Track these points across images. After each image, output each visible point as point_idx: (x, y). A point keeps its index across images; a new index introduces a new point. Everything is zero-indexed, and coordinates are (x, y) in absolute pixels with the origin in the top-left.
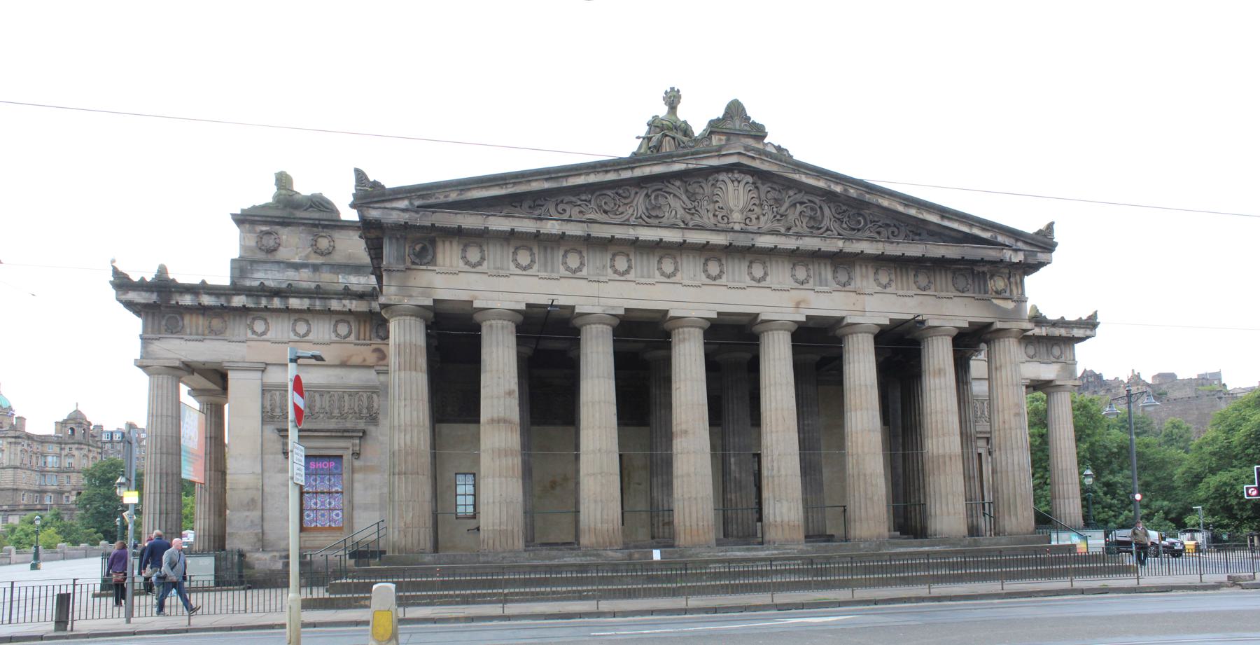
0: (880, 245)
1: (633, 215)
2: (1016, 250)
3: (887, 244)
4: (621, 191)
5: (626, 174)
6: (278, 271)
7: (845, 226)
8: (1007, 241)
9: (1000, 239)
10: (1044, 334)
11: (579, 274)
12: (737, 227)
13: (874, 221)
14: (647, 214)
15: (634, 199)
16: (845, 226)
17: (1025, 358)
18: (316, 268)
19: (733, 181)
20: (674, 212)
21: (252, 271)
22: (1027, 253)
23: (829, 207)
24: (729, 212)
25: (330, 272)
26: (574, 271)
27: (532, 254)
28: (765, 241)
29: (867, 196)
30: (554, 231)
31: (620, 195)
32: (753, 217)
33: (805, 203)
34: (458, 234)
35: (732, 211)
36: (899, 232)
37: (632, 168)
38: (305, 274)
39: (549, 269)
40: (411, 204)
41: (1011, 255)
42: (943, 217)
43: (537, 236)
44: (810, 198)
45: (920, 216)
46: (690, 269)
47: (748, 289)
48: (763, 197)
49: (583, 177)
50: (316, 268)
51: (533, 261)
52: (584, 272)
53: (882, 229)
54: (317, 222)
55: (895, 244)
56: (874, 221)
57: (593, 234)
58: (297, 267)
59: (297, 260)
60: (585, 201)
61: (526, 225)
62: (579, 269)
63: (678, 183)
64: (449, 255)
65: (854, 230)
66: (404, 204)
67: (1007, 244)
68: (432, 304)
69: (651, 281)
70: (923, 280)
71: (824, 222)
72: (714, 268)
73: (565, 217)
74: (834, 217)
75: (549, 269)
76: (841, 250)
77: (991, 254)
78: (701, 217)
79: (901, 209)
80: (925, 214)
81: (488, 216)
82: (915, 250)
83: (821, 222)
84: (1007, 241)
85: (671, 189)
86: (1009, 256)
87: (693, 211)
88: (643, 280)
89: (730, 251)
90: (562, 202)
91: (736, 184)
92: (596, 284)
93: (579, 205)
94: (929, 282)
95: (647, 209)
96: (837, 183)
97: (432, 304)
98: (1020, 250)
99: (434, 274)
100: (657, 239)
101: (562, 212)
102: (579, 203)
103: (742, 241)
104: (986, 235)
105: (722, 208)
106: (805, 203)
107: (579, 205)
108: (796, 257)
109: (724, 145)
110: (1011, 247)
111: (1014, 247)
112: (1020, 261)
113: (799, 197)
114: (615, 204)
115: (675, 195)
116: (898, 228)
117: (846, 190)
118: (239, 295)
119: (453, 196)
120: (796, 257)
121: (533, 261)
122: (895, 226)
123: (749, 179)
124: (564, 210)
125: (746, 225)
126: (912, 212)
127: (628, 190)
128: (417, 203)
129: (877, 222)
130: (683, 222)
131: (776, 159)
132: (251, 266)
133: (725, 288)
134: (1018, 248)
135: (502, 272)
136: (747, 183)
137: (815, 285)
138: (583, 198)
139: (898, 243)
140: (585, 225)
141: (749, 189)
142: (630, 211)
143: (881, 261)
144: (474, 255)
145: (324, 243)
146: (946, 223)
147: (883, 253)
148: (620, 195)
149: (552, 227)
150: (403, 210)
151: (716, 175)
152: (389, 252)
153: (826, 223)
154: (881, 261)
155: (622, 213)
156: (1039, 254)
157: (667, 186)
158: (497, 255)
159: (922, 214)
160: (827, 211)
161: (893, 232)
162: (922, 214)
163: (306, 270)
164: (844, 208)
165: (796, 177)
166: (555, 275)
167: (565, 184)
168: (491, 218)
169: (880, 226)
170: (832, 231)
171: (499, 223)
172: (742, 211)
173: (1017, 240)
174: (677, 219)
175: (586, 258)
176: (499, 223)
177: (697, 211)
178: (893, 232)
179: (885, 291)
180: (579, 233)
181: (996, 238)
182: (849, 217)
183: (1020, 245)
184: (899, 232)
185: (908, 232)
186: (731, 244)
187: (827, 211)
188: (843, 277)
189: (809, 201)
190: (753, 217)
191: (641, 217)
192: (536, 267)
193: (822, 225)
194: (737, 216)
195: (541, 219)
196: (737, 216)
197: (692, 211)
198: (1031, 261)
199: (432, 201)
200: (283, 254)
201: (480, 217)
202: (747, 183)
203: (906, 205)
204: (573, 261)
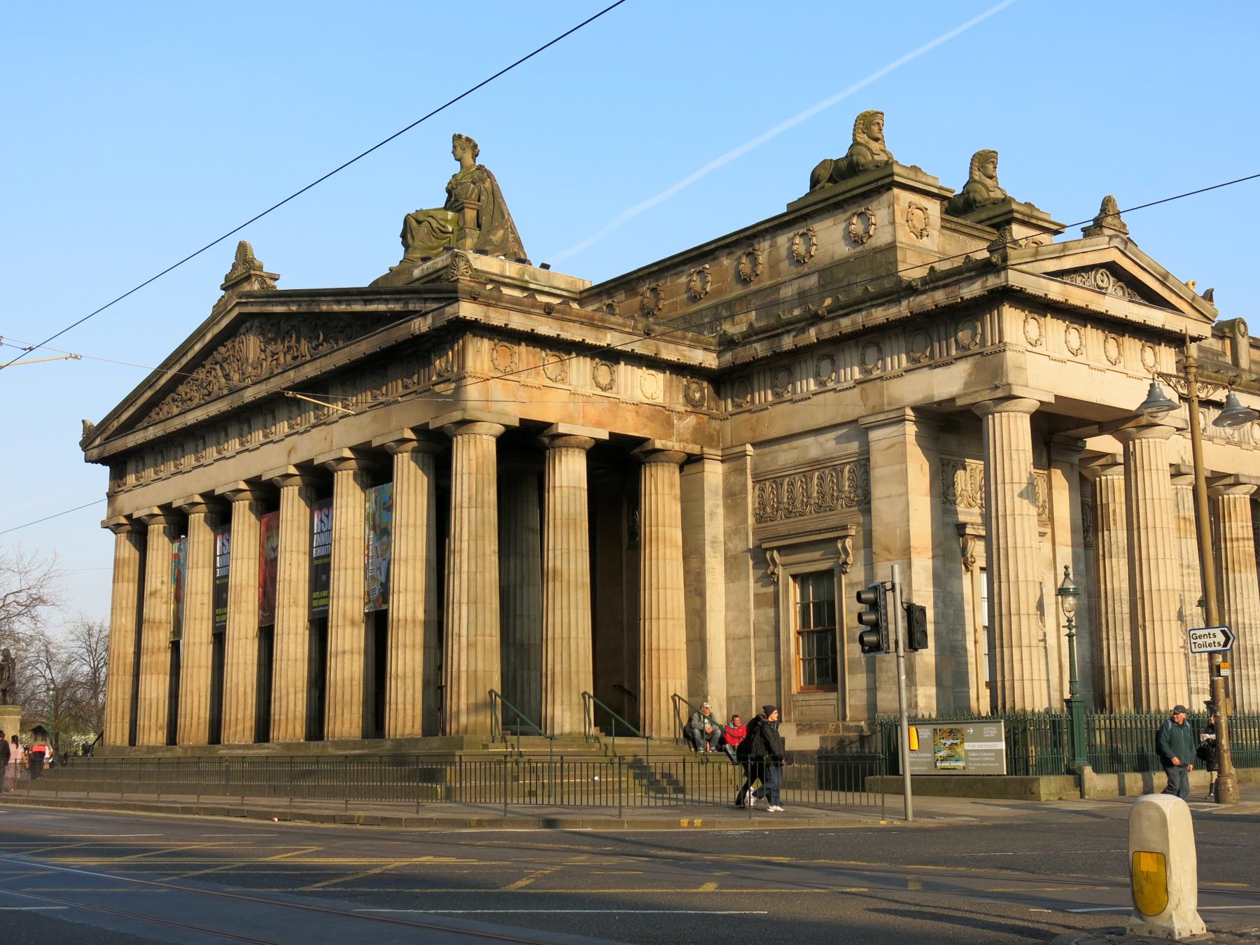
2: (425, 314)
28: (250, 395)
37: (186, 353)
45: (349, 309)
68: (518, 425)
79: (335, 308)
97: (518, 425)
119: (116, 424)
123: (256, 323)
126: (343, 308)
128: (104, 436)
199: (108, 433)
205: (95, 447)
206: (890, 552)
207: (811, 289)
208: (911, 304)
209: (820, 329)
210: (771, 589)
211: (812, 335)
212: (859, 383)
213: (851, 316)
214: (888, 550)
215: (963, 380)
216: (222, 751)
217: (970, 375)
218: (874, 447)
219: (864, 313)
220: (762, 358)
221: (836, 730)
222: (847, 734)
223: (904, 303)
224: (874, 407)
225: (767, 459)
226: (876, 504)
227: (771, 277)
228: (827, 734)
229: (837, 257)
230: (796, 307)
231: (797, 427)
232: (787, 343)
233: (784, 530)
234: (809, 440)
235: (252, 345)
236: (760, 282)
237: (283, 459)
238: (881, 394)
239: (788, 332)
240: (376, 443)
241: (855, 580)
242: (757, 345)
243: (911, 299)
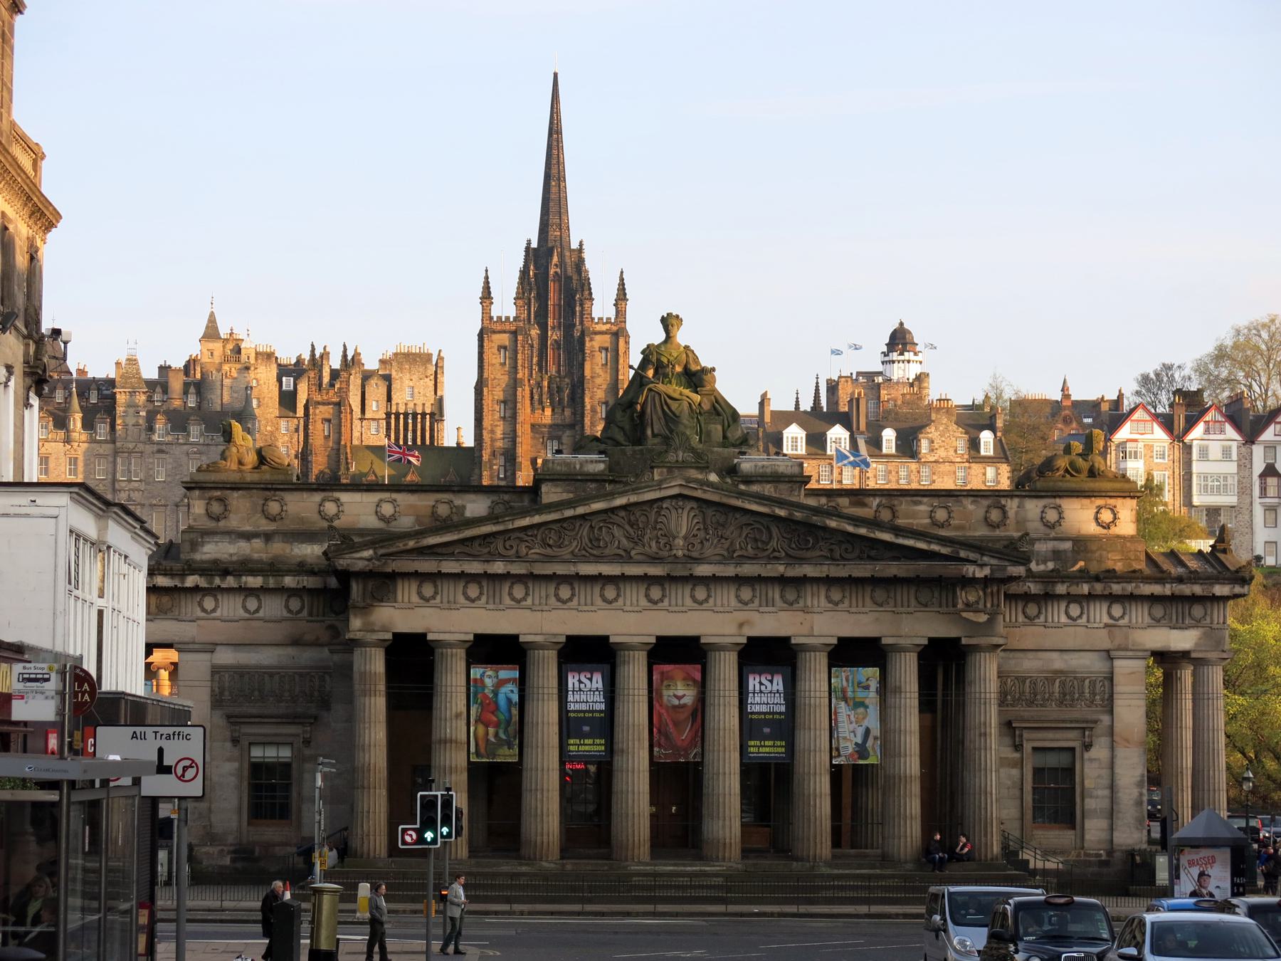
0: (825, 568)
1: (577, 546)
2: (982, 566)
3: (832, 567)
4: (565, 525)
5: (569, 513)
6: (229, 543)
7: (794, 546)
8: (972, 556)
9: (963, 554)
10: (1168, 592)
11: (524, 603)
12: (680, 553)
13: (826, 539)
14: (590, 545)
15: (579, 531)
16: (794, 546)
17: (1147, 619)
18: (268, 537)
19: (676, 509)
20: (617, 542)
21: (203, 544)
22: (994, 567)
23: (778, 527)
24: (671, 539)
25: (283, 542)
26: (518, 601)
27: (481, 587)
28: (703, 570)
29: (814, 518)
30: (500, 571)
31: (565, 528)
32: (696, 541)
33: (752, 525)
34: (416, 575)
35: (674, 538)
36: (853, 548)
38: (258, 543)
39: (497, 600)
40: (375, 553)
41: (974, 571)
42: (897, 535)
43: (486, 575)
44: (757, 519)
45: (872, 535)
46: (633, 595)
47: (690, 613)
48: (708, 522)
49: (528, 519)
50: (268, 537)
51: (481, 594)
52: (529, 601)
53: (833, 547)
54: (270, 486)
55: (841, 566)
56: (826, 539)
57: (536, 572)
58: (248, 536)
59: (248, 528)
60: (532, 536)
61: (475, 567)
62: (524, 599)
63: (623, 513)
64: (407, 592)
65: (803, 549)
66: (368, 553)
67: (971, 559)
69: (593, 608)
70: (880, 594)
71: (771, 544)
72: (656, 593)
73: (513, 552)
74: (783, 537)
75: (497, 600)
76: (782, 576)
77: (951, 569)
78: (644, 546)
79: (850, 529)
80: (877, 533)
81: (441, 560)
82: (862, 570)
83: (767, 544)
84: (972, 556)
85: (615, 518)
86: (970, 570)
87: (636, 540)
88: (586, 608)
89: (671, 579)
90: (509, 538)
91: (680, 511)
92: (539, 613)
93: (526, 541)
94: (888, 597)
95: (591, 541)
96: (782, 508)
98: (986, 565)
99: (392, 609)
100: (596, 573)
101: (508, 547)
102: (527, 538)
103: (679, 571)
104: (944, 550)
105: (665, 536)
106: (752, 525)
107: (526, 541)
108: (739, 580)
109: (665, 480)
110: (975, 562)
111: (979, 562)
112: (986, 576)
113: (745, 519)
114: (560, 538)
115: (618, 525)
116: (852, 544)
117: (790, 514)
118: (193, 575)
119: (411, 544)
120: (739, 580)
121: (481, 594)
122: (848, 541)
123: (694, 505)
124: (512, 547)
125: (688, 550)
126: (863, 531)
127: (572, 523)
129: (830, 539)
130: (625, 550)
131: (717, 489)
132: (202, 538)
133: (665, 612)
134: (982, 562)
135: (453, 606)
136: (692, 508)
137: (760, 606)
138: (530, 534)
139: (844, 565)
140: (528, 564)
141: (693, 514)
142: (575, 544)
143: (829, 581)
144: (428, 590)
145: (274, 507)
146: (901, 541)
147: (828, 576)
148: (565, 528)
149: (498, 567)
150: (369, 560)
151: (660, 503)
152: (356, 588)
153: (774, 543)
154: (829, 581)
155: (566, 546)
156: (1009, 568)
157: (610, 518)
158: (451, 591)
159: (874, 533)
160: (775, 531)
161: (847, 549)
162: (874, 533)
163: (258, 541)
164: (793, 527)
165: (739, 503)
166: (501, 607)
167: (511, 527)
168: (444, 563)
169: (832, 544)
170: (779, 552)
171: (450, 567)
172: (685, 538)
173: (983, 555)
174: (619, 548)
175: (531, 589)
176: (450, 567)
177: (640, 540)
178: (847, 549)
179: (836, 608)
180: (523, 571)
181: (958, 553)
182: (799, 536)
183: (985, 559)
184: (853, 548)
185: (864, 548)
186: (668, 575)
187: (775, 531)
188: (791, 595)
189: (755, 521)
190: (696, 541)
191: (585, 549)
192: (484, 599)
193: (768, 547)
194: (680, 542)
195: (488, 561)
196: (680, 542)
197: (636, 541)
198: (998, 575)
200: (234, 522)
201: (434, 562)
202: (692, 508)
203: (856, 526)
204: (519, 591)
205: (361, 559)
206: (1128, 742)
207: (1065, 551)
208: (1174, 589)
209: (1093, 587)
210: (1017, 755)
211: (1085, 589)
212: (1106, 626)
213: (1122, 584)
214: (1127, 741)
215: (1194, 642)
216: (632, 868)
217: (1200, 639)
218: (1116, 671)
219: (1134, 585)
220: (1034, 595)
221: (1079, 855)
222: (1087, 859)
223: (1168, 586)
224: (1120, 645)
225: (1012, 662)
226: (1116, 709)
227: (1018, 531)
228: (1070, 858)
229: (1083, 532)
230: (1050, 561)
231: (1047, 645)
232: (1061, 589)
233: (1026, 715)
234: (1055, 655)
235: (682, 523)
236: (1007, 531)
237: (731, 629)
238: (1127, 638)
239: (1063, 582)
240: (884, 641)
241: (1094, 757)
242: (1032, 586)
243: (1174, 585)
